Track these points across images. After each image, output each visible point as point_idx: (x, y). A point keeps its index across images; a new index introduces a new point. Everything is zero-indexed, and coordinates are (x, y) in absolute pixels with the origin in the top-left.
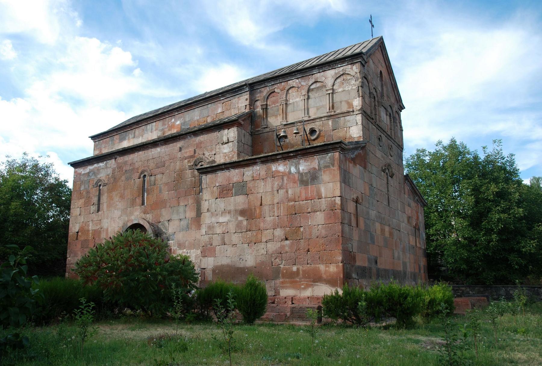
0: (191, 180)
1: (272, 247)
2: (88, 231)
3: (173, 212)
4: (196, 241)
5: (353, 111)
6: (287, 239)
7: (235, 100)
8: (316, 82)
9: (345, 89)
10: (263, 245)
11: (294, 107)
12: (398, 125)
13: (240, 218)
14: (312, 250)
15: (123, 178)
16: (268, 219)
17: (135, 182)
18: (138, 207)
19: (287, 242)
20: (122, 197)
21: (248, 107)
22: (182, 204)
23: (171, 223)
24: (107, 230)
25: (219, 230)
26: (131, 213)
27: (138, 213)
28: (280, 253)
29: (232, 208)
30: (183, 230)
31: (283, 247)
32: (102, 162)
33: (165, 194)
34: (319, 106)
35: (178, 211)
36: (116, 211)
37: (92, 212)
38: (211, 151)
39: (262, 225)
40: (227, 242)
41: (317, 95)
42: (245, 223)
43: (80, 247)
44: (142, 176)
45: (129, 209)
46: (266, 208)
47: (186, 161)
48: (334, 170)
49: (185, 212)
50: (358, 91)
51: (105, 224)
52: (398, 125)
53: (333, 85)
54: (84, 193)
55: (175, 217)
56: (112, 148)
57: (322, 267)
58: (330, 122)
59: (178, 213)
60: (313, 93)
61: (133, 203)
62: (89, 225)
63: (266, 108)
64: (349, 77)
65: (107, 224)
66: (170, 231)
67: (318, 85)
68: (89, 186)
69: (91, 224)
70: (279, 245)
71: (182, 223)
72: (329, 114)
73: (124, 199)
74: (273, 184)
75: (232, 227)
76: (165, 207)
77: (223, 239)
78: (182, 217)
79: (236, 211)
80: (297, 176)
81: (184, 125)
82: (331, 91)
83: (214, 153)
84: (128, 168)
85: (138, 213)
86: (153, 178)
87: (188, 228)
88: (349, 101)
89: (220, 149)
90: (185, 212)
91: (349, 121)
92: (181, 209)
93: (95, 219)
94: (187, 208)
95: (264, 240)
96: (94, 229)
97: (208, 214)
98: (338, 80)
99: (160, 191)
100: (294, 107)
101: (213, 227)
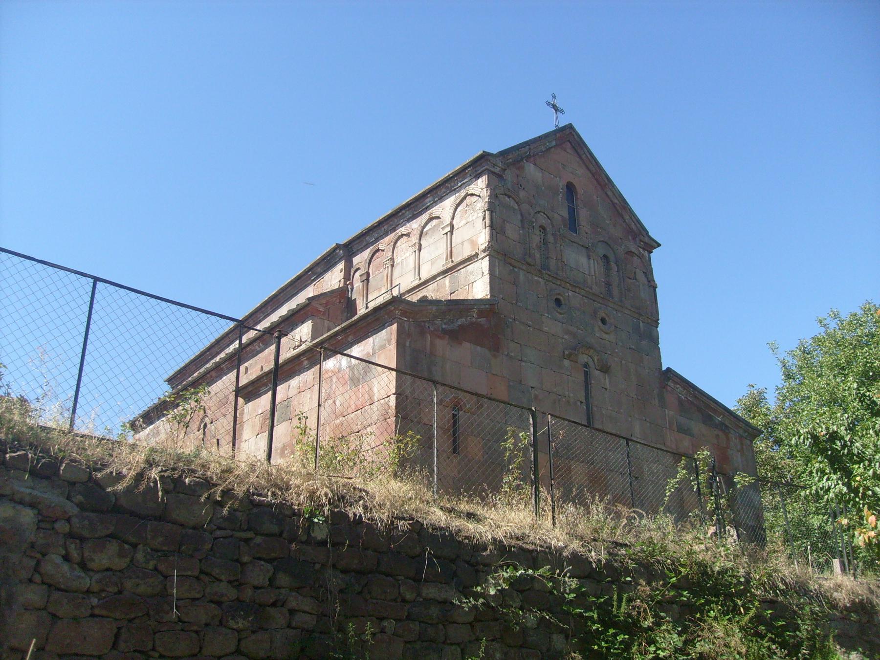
5: (477, 254)
7: (328, 276)
8: (431, 219)
9: (468, 220)
11: (402, 268)
12: (641, 277)
21: (342, 281)
34: (434, 256)
41: (431, 240)
48: (390, 350)
50: (484, 218)
52: (641, 277)
53: (453, 218)
58: (447, 281)
60: (427, 237)
63: (368, 279)
64: (474, 199)
67: (435, 222)
72: (445, 268)
80: (348, 370)
82: (448, 229)
88: (474, 238)
91: (472, 273)
98: (459, 209)
100: (402, 268)
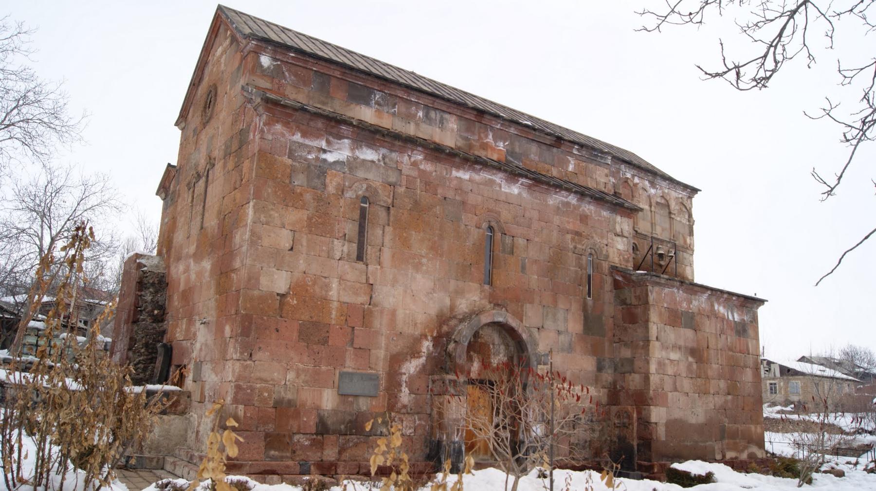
0: (576, 272)
1: (719, 400)
2: (326, 300)
3: (547, 315)
4: (582, 373)
6: (729, 394)
10: (711, 398)
13: (690, 359)
14: (746, 409)
15: (438, 210)
16: (715, 366)
17: (468, 232)
18: (475, 285)
19: (730, 397)
20: (435, 249)
22: (561, 305)
23: (543, 334)
24: (393, 313)
25: (670, 371)
26: (459, 292)
27: (476, 298)
28: (724, 409)
29: (681, 343)
30: (563, 350)
31: (726, 402)
32: (372, 145)
33: (534, 279)
35: (554, 315)
36: (419, 276)
37: (338, 255)
38: (602, 237)
39: (710, 373)
40: (679, 389)
42: (695, 366)
43: (295, 335)
44: (485, 225)
45: (453, 285)
46: (712, 352)
47: (569, 236)
49: (566, 320)
51: (389, 296)
54: (308, 197)
55: (549, 324)
56: (324, 104)
57: (753, 427)
59: (555, 320)
61: (464, 272)
62: (327, 287)
65: (391, 299)
66: (542, 348)
68: (325, 185)
69: (335, 285)
70: (723, 399)
71: (562, 338)
73: (441, 256)
74: (716, 326)
75: (683, 369)
76: (532, 302)
77: (675, 383)
78: (562, 328)
79: (686, 348)
81: (512, 157)
83: (605, 242)
84: (450, 194)
85: (476, 298)
86: (508, 240)
87: (570, 349)
89: (612, 239)
90: (566, 320)
92: (561, 315)
93: (348, 277)
94: (570, 316)
95: (712, 392)
96: (346, 299)
97: (657, 344)
99: (523, 268)
101: (664, 364)
